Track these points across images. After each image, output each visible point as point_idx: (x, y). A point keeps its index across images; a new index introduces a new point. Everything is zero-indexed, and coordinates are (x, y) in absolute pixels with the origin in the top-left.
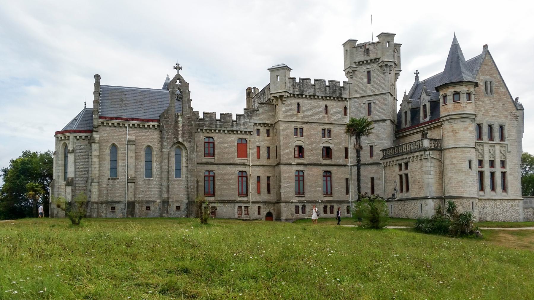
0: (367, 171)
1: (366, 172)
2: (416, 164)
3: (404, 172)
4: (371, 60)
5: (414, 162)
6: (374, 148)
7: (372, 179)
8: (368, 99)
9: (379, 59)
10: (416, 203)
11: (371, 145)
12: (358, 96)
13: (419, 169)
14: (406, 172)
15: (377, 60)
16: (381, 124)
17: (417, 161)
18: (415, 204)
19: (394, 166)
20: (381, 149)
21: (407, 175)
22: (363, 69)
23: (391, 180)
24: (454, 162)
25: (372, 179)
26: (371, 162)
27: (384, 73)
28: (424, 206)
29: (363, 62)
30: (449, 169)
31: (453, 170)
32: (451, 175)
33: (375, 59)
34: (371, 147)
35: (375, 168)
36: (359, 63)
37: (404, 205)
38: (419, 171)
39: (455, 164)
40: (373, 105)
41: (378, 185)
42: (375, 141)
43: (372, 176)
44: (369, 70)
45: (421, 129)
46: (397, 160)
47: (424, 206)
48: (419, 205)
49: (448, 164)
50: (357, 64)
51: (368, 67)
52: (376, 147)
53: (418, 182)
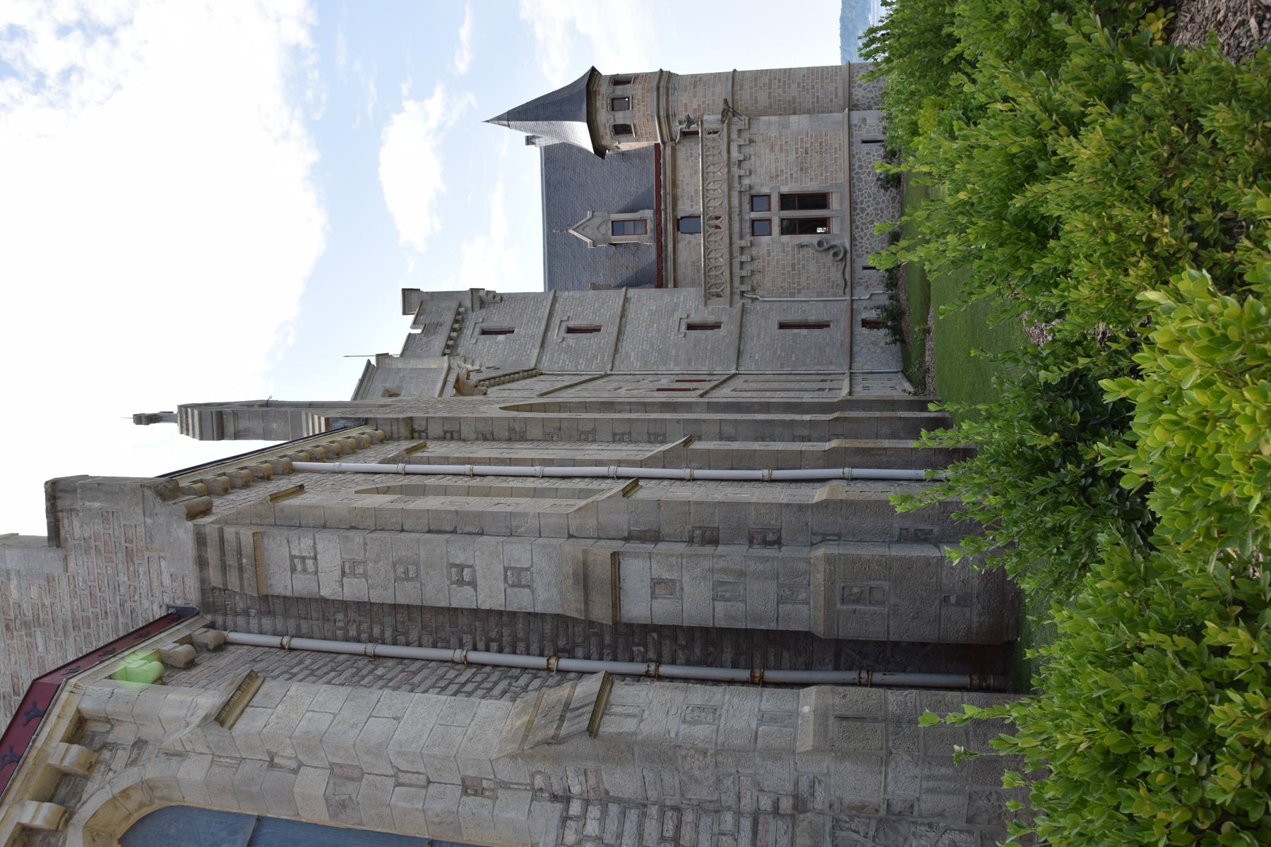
0: (759, 335)
1: (762, 336)
2: (758, 162)
3: (776, 215)
4: (456, 321)
5: (753, 168)
6: (695, 319)
7: (782, 326)
8: (555, 335)
9: (460, 306)
10: (860, 160)
11: (683, 328)
12: (536, 352)
13: (772, 150)
14: (775, 201)
15: (462, 310)
16: (632, 307)
17: (753, 158)
18: (861, 167)
19: (754, 251)
20: (701, 307)
21: (787, 201)
22: (469, 340)
23: (793, 266)
24: (767, 81)
25: (782, 326)
26: (734, 328)
27: (501, 300)
28: (869, 131)
29: (450, 338)
30: (781, 91)
31: (784, 82)
32: (794, 86)
33: (458, 313)
34: (691, 327)
35: (752, 319)
36: (447, 346)
37: (863, 210)
38: (777, 148)
39: (770, 80)
40: (572, 324)
41: (804, 312)
42: (676, 317)
43: (777, 326)
44: (477, 330)
45: (670, 226)
46: (741, 237)
47: (869, 131)
48: (866, 147)
49: (770, 97)
50: (447, 351)
51: (467, 332)
52: (692, 315)
53: (807, 153)
